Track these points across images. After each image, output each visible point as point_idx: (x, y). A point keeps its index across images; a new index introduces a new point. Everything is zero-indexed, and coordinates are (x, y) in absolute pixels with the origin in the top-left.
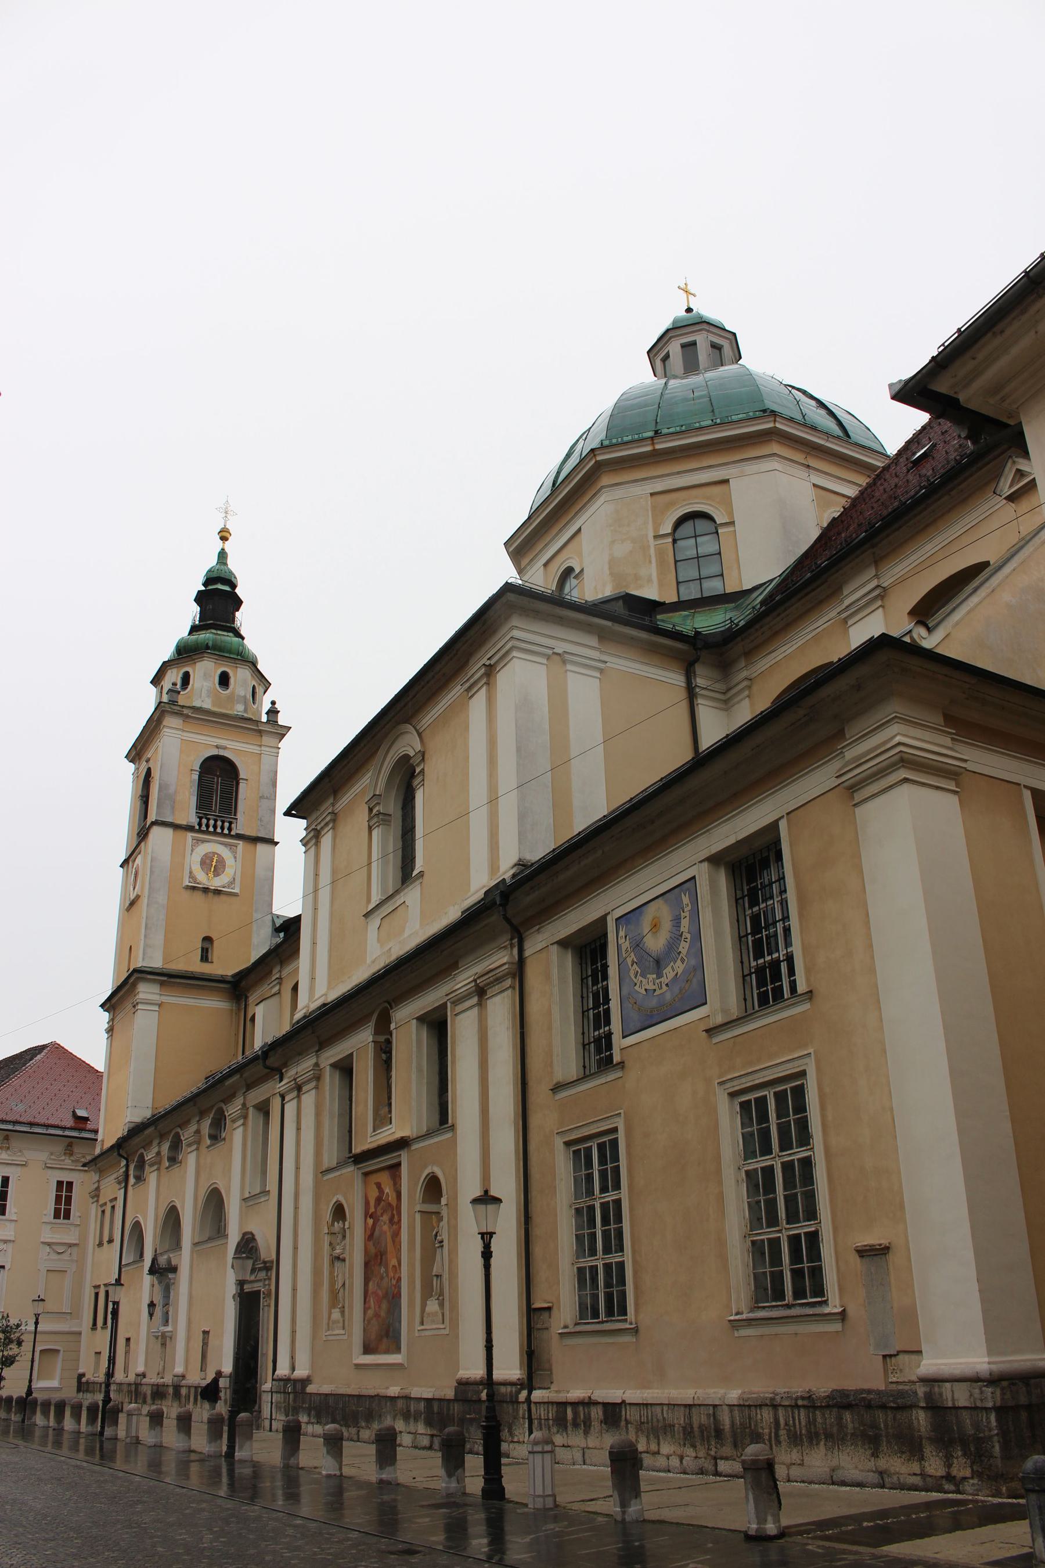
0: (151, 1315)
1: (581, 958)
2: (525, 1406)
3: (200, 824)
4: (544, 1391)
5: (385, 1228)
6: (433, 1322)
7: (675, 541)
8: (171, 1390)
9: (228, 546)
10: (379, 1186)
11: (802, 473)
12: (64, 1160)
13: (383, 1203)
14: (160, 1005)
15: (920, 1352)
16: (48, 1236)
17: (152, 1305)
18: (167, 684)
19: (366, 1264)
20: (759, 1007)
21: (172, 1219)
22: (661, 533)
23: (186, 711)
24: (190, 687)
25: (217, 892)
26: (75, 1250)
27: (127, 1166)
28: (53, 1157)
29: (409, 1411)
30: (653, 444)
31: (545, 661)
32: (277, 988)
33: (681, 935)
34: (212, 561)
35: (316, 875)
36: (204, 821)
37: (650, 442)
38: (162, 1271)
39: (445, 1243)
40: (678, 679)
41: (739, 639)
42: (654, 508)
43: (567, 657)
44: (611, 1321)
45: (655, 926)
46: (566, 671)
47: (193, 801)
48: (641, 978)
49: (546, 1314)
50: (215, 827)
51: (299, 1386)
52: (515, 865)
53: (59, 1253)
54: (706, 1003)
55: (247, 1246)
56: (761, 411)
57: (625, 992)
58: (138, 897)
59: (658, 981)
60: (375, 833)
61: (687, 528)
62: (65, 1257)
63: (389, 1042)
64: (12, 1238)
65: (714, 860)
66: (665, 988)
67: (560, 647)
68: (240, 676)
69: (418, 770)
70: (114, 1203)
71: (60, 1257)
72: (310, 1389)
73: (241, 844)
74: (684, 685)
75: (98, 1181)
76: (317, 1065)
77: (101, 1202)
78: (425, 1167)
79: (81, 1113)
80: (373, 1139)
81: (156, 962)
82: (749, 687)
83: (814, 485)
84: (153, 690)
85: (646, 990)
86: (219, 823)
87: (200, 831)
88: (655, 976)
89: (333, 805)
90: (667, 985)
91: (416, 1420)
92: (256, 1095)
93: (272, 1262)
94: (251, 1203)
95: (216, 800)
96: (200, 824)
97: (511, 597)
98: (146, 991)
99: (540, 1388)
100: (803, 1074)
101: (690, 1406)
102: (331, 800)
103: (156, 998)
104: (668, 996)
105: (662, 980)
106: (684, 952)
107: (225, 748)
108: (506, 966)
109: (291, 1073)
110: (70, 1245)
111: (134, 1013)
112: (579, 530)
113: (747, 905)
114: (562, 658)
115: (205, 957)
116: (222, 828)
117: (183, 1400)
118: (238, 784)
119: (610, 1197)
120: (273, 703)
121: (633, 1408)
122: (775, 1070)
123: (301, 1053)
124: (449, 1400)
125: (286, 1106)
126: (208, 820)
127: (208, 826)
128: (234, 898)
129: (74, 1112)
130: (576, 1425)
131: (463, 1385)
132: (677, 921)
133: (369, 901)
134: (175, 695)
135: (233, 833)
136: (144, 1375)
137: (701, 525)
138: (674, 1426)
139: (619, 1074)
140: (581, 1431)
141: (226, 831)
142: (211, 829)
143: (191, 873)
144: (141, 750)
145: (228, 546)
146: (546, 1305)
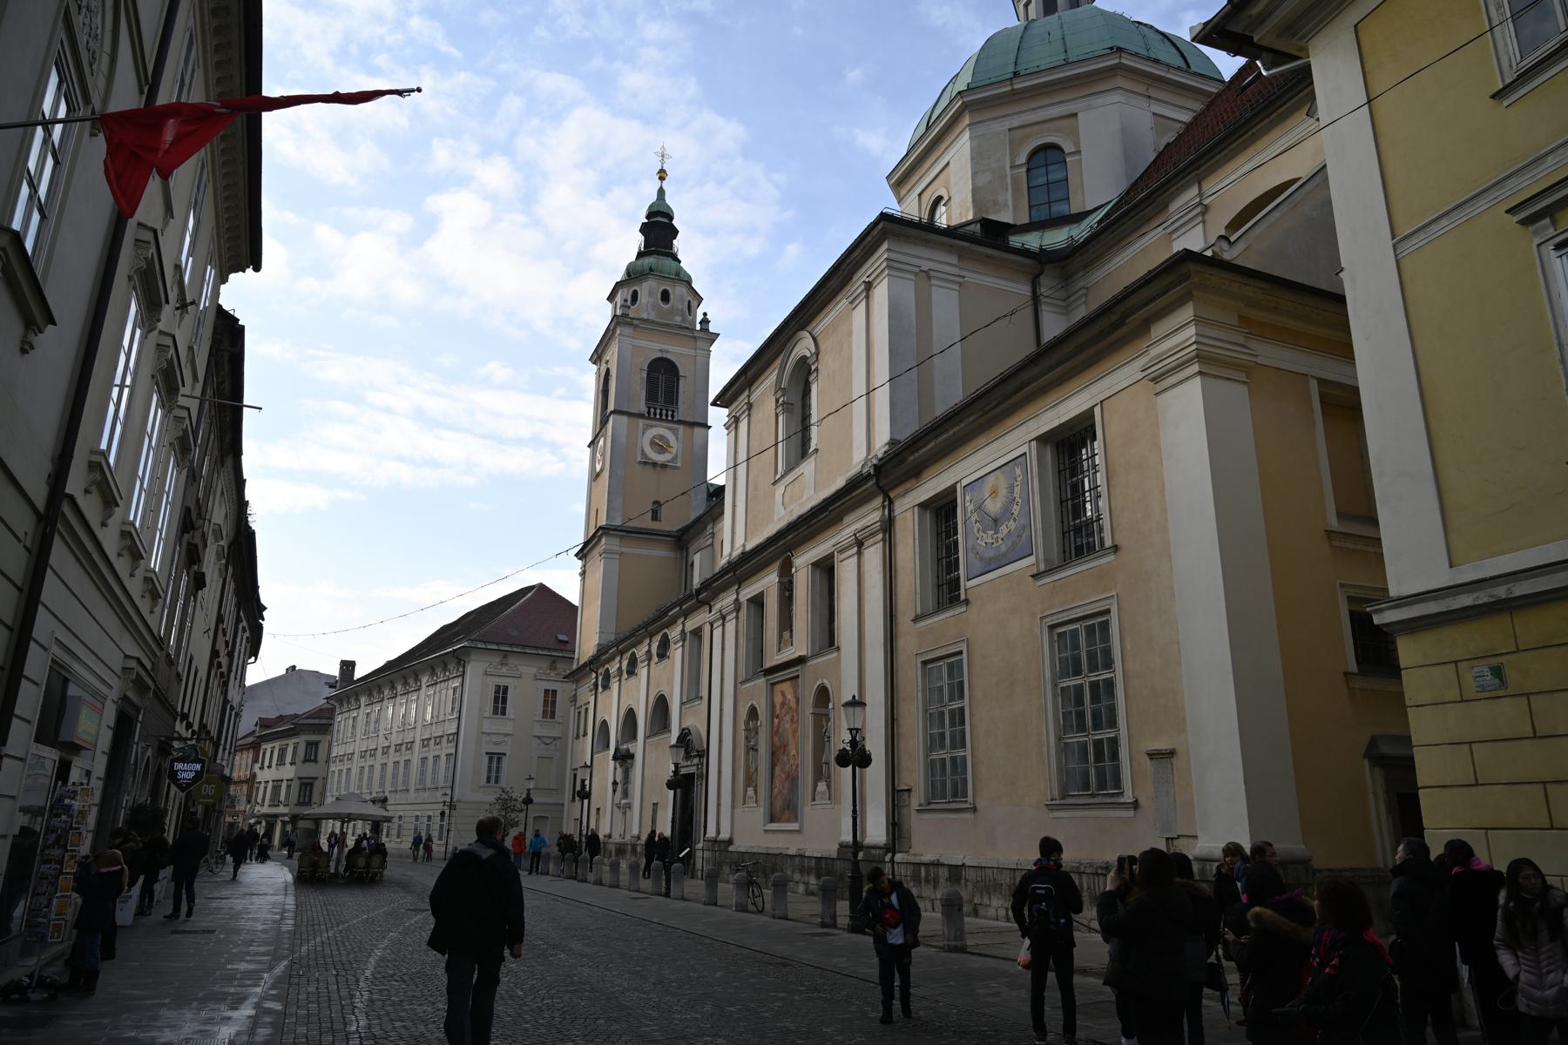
0: (614, 791)
1: (937, 518)
2: (890, 864)
3: (649, 413)
4: (905, 854)
5: (787, 726)
6: (822, 798)
7: (1028, 170)
8: (629, 847)
9: (665, 185)
10: (783, 694)
11: (1143, 103)
12: (549, 674)
13: (786, 707)
14: (620, 554)
15: (1196, 837)
16: (538, 731)
17: (615, 783)
18: (618, 299)
19: (773, 754)
20: (1076, 557)
21: (631, 715)
22: (1017, 163)
23: (635, 322)
25: (664, 466)
26: (559, 741)
27: (597, 678)
28: (541, 671)
29: (803, 867)
30: (1012, 84)
31: (913, 277)
32: (711, 540)
33: (1014, 500)
34: (654, 198)
35: (736, 452)
36: (652, 410)
37: (1009, 83)
38: (624, 758)
39: (832, 738)
40: (1025, 290)
41: (1078, 254)
42: (1011, 142)
43: (931, 273)
44: (956, 802)
45: (994, 492)
46: (931, 285)
48: (982, 534)
49: (906, 794)
52: (888, 443)
53: (547, 744)
54: (1032, 554)
55: (685, 738)
57: (969, 544)
58: (602, 470)
59: (995, 536)
60: (780, 419)
61: (1041, 156)
62: (552, 747)
63: (791, 582)
65: (1042, 439)
66: (1000, 541)
67: (926, 266)
68: (677, 291)
69: (813, 368)
73: (681, 428)
74: (1029, 294)
75: (576, 690)
76: (737, 600)
77: (578, 705)
78: (818, 679)
79: (562, 637)
80: (778, 657)
81: (618, 522)
82: (1086, 295)
83: (1154, 114)
84: (609, 306)
85: (986, 543)
86: (664, 412)
87: (649, 418)
88: (993, 532)
89: (749, 396)
90: (1002, 539)
91: (808, 874)
92: (691, 624)
93: (703, 751)
94: (688, 706)
97: (888, 225)
99: (900, 852)
100: (1108, 612)
102: (746, 393)
104: (1003, 549)
105: (999, 535)
106: (1016, 513)
107: (667, 352)
108: (878, 524)
110: (555, 738)
112: (948, 163)
113: (1068, 476)
114: (928, 275)
115: (655, 516)
116: (667, 416)
118: (678, 380)
119: (956, 705)
120: (705, 314)
121: (972, 870)
122: (1086, 608)
123: (724, 588)
124: (833, 859)
125: (714, 631)
126: (655, 409)
127: (655, 414)
128: (676, 471)
129: (556, 637)
130: (927, 881)
131: (842, 846)
132: (1011, 488)
133: (776, 473)
134: (627, 309)
135: (675, 419)
136: (610, 836)
137: (1051, 154)
138: (1001, 885)
139: (964, 609)
140: (932, 886)
141: (670, 418)
142: (658, 416)
143: (643, 451)
144: (601, 353)
145: (665, 185)
146: (906, 788)
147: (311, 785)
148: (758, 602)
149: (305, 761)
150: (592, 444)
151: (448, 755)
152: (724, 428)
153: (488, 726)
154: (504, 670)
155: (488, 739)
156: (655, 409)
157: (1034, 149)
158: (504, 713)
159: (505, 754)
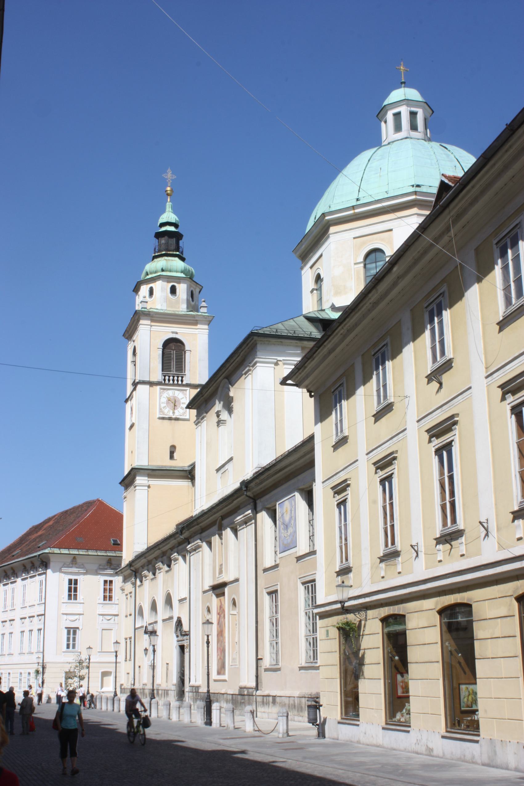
2: (255, 697)
3: (165, 380)
7: (365, 265)
14: (149, 487)
24: (154, 296)
29: (227, 699)
36: (167, 378)
49: (261, 660)
50: (173, 380)
51: (197, 689)
56: (411, 186)
62: (112, 621)
64: (82, 613)
70: (127, 596)
71: (109, 622)
77: (126, 593)
86: (176, 378)
87: (165, 384)
95: (173, 364)
96: (165, 380)
101: (289, 697)
104: (289, 541)
107: (177, 333)
111: (135, 491)
112: (321, 256)
117: (160, 696)
121: (279, 697)
126: (169, 377)
127: (169, 380)
132: (291, 510)
135: (184, 383)
137: (378, 254)
141: (180, 382)
142: (171, 382)
151: (39, 630)
152: (194, 424)
155: (65, 617)
156: (169, 377)
157: (369, 250)
158: (76, 598)
159: (78, 628)
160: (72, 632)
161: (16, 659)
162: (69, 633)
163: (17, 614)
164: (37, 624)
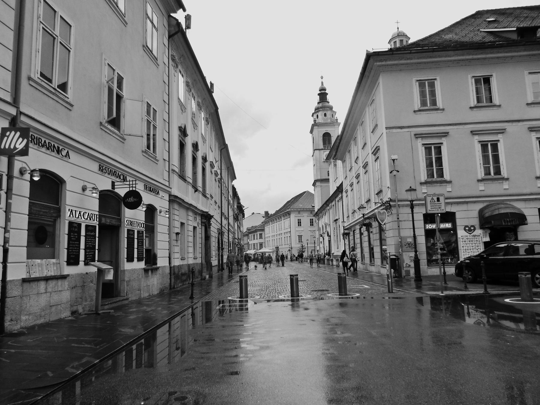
3: (324, 148)
9: (323, 80)
47: (322, 143)
68: (329, 113)
72: (334, 254)
79: (313, 205)
81: (319, 178)
87: (324, 149)
98: (318, 184)
103: (320, 185)
109: (330, 205)
110: (314, 231)
145: (323, 80)
147: (262, 244)
148: (333, 205)
149: (260, 238)
150: (312, 156)
151: (289, 236)
153: (297, 229)
154: (299, 215)
155: (297, 232)
158: (301, 225)
160: (300, 237)
161: (284, 246)
162: (299, 237)
163: (283, 232)
164: (289, 235)
